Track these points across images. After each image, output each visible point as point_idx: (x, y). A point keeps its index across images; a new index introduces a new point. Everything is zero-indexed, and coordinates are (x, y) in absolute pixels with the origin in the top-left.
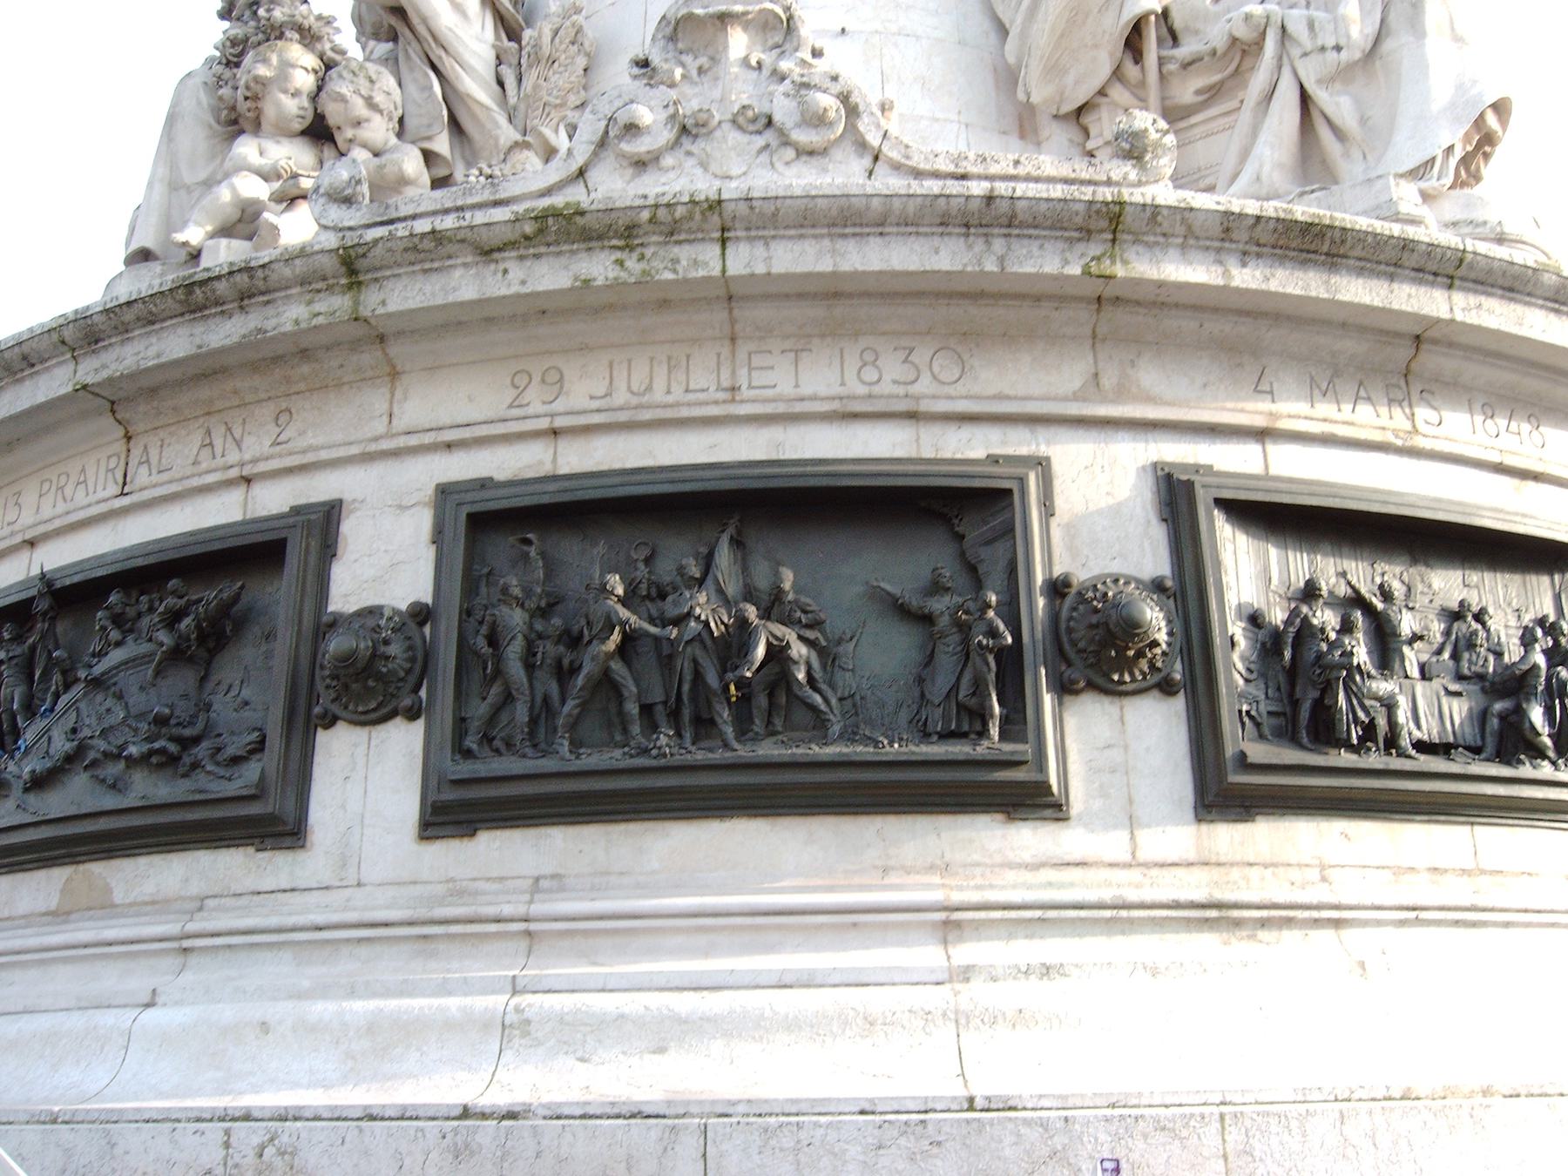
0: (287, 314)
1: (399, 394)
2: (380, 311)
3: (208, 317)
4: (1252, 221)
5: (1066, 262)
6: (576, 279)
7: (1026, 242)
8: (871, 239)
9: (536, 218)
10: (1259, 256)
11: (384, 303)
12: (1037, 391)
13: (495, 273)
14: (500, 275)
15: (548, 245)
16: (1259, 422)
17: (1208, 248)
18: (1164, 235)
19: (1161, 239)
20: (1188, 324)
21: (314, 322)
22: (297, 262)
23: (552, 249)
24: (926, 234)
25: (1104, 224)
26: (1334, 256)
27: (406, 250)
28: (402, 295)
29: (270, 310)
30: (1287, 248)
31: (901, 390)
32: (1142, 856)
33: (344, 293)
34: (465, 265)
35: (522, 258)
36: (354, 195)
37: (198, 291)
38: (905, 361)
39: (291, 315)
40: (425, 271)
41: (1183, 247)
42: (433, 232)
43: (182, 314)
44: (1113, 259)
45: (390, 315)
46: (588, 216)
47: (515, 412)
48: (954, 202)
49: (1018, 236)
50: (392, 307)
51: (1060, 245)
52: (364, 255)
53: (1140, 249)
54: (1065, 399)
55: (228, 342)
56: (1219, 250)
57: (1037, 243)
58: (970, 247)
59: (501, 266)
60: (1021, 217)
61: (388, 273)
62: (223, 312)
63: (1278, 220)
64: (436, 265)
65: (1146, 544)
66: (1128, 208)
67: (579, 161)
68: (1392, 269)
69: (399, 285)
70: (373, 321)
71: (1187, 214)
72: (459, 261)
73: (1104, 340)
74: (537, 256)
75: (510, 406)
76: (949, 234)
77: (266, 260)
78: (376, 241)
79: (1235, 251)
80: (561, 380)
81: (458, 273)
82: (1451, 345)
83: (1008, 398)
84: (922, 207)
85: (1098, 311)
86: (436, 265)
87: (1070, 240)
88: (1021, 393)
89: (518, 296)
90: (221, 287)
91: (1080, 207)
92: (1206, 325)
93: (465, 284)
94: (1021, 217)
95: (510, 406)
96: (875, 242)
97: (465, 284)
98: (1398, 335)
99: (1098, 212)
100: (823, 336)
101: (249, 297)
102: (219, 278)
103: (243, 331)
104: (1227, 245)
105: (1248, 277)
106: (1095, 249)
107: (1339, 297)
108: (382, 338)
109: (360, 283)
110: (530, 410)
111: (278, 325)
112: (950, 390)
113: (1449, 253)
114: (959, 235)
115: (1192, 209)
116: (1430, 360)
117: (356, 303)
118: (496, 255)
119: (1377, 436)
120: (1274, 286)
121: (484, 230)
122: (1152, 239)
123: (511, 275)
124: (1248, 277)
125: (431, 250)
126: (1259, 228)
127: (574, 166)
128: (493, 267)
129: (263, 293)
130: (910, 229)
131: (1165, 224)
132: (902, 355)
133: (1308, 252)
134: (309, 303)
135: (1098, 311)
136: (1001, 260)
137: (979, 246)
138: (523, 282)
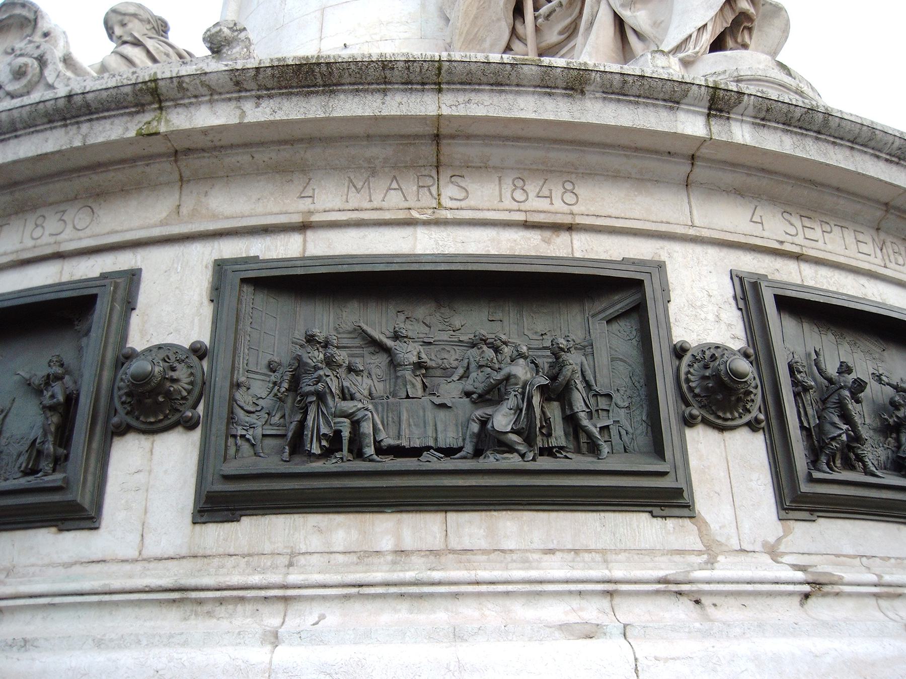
4: (253, 73)
5: (127, 129)
7: (102, 122)
8: (11, 141)
10: (270, 97)
12: (136, 223)
16: (297, 219)
17: (230, 99)
18: (196, 97)
19: (193, 100)
20: (242, 158)
24: (42, 131)
25: (149, 98)
26: (330, 85)
30: (291, 87)
31: (52, 240)
32: (146, 553)
38: (61, 220)
41: (211, 102)
44: (159, 121)
48: (48, 104)
49: (97, 119)
51: (125, 119)
53: (180, 110)
54: (155, 226)
56: (239, 99)
57: (109, 121)
58: (67, 133)
60: (93, 106)
63: (272, 67)
65: (196, 320)
66: (161, 83)
68: (383, 86)
71: (203, 78)
73: (189, 181)
76: (55, 127)
79: (252, 96)
82: (468, 137)
83: (117, 232)
84: (31, 113)
85: (176, 161)
87: (131, 114)
88: (125, 228)
91: (128, 90)
92: (256, 156)
94: (93, 106)
96: (13, 142)
98: (417, 136)
99: (141, 90)
100: (17, 213)
104: (243, 94)
105: (259, 113)
106: (148, 117)
107: (335, 114)
112: (81, 234)
113: (426, 65)
114: (61, 126)
115: (206, 73)
116: (454, 151)
119: (401, 215)
120: (279, 116)
122: (186, 101)
124: (259, 113)
126: (261, 76)
130: (32, 130)
131: (191, 88)
132: (59, 216)
133: (309, 86)
135: (176, 161)
136: (85, 137)
137: (73, 130)
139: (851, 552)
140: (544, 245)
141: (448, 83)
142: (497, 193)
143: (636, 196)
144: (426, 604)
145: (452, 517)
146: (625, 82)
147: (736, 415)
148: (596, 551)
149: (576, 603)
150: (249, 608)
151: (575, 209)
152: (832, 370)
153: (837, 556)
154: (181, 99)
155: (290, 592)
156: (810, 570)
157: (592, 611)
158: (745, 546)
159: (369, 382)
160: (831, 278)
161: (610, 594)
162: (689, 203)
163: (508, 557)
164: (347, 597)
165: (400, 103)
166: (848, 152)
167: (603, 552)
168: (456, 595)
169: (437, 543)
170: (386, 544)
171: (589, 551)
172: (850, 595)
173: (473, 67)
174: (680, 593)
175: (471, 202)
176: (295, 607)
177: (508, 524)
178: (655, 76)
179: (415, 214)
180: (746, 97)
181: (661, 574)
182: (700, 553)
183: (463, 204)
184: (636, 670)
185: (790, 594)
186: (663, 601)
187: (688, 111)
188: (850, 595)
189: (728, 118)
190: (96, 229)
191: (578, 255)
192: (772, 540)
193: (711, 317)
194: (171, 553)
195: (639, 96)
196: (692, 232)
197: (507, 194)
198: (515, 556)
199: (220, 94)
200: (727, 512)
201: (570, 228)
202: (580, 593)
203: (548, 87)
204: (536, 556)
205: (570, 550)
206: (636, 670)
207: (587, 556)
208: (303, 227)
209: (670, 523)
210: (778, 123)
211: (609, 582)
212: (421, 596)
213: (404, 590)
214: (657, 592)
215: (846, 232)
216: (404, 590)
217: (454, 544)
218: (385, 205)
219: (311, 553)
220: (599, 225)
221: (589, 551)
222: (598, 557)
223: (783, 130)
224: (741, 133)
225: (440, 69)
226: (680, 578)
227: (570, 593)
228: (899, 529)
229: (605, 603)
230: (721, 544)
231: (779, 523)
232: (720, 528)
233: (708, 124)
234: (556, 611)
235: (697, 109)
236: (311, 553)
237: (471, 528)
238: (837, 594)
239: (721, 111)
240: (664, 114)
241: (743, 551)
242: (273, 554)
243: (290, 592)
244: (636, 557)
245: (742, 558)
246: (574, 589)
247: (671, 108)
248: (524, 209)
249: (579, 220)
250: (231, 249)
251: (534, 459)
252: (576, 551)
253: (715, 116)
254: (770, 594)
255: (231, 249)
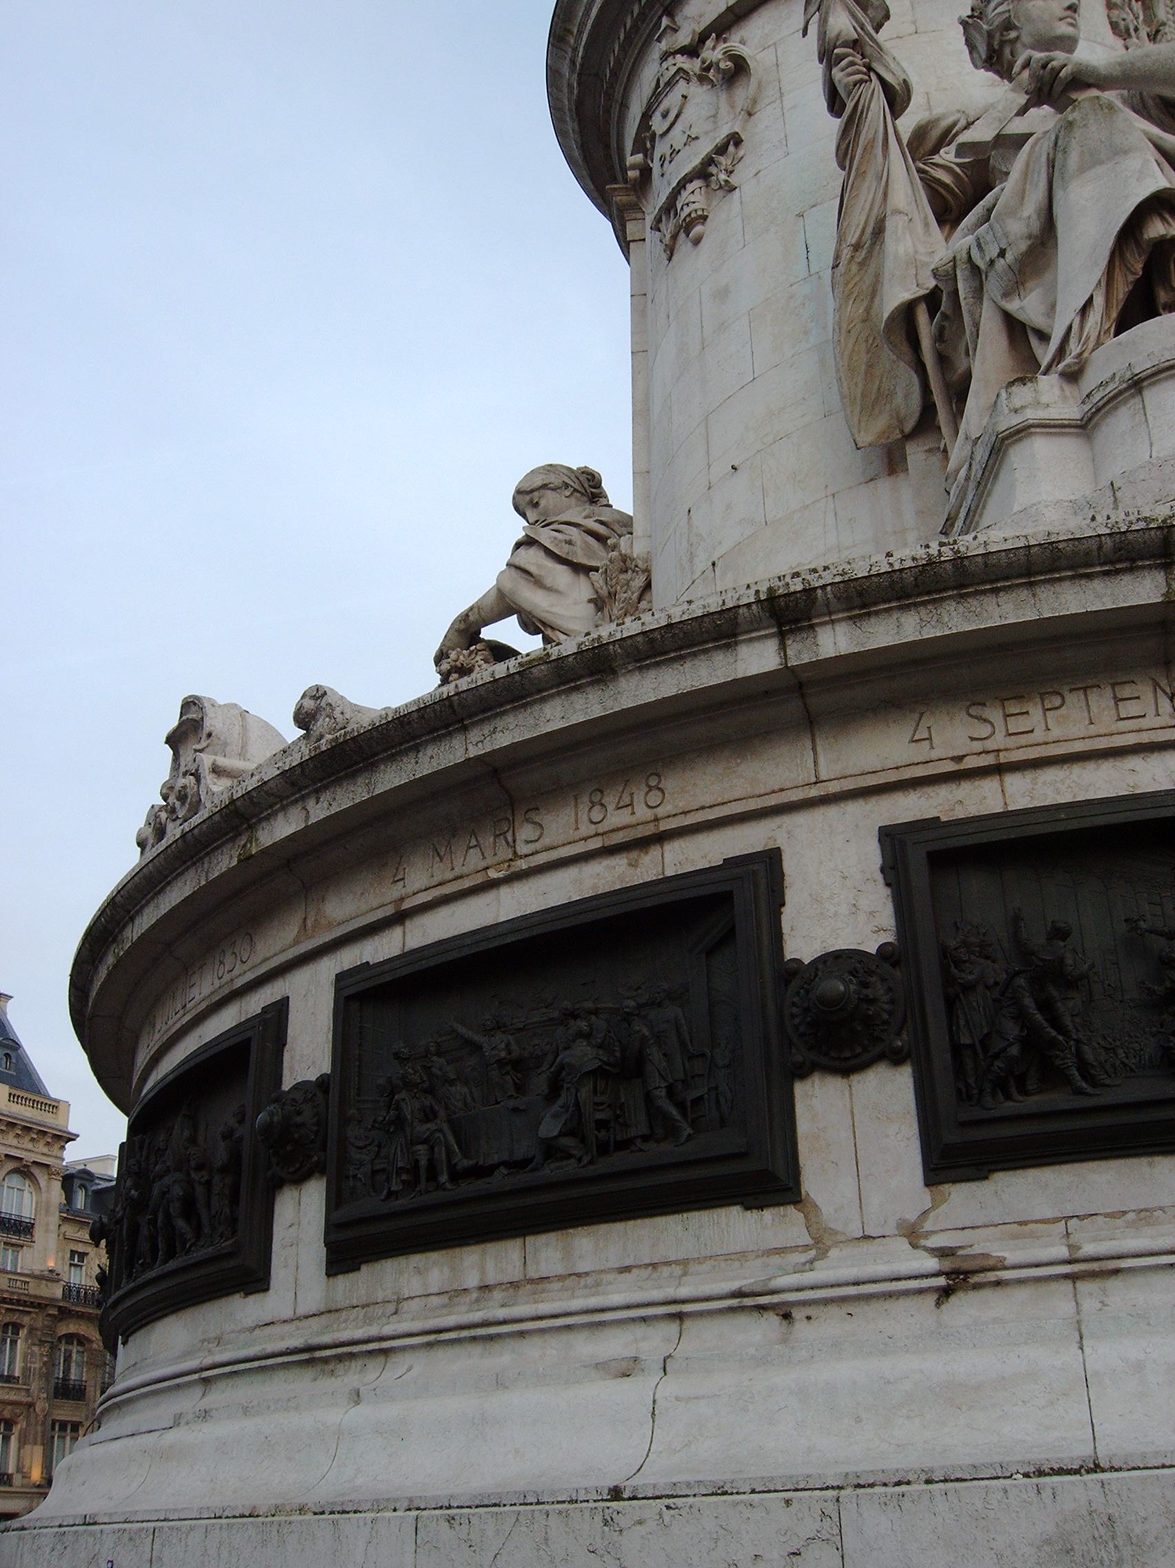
4: (299, 770)
105: (319, 810)
124: (319, 810)
139: (1049, 1214)
140: (631, 870)
141: (470, 717)
142: (573, 819)
143: (738, 765)
144: (496, 1346)
145: (530, 1240)
146: (652, 641)
147: (859, 1050)
148: (677, 1262)
149: (640, 1330)
150: (360, 1362)
151: (660, 811)
152: (1037, 938)
153: (1021, 1223)
154: (262, 812)
155: (385, 1345)
156: (960, 1252)
157: (653, 1342)
158: (870, 1231)
159: (465, 1090)
160: (1063, 781)
161: (680, 1317)
162: (814, 749)
163: (582, 1281)
164: (429, 1345)
165: (432, 757)
166: (1024, 594)
167: (685, 1263)
168: (522, 1334)
169: (515, 1273)
170: (472, 1280)
171: (668, 1263)
172: (1020, 1282)
173: (482, 691)
174: (761, 1308)
175: (546, 841)
176: (396, 1359)
177: (584, 1241)
178: (685, 617)
179: (493, 874)
180: (819, 591)
181: (734, 1285)
182: (807, 1248)
183: (538, 846)
184: (653, 1413)
185: (920, 1291)
186: (742, 1320)
187: (751, 640)
188: (1020, 1282)
189: (812, 627)
190: (256, 959)
191: (670, 872)
192: (912, 1216)
193: (844, 909)
194: (314, 1310)
195: (681, 648)
196: (814, 792)
197: (584, 817)
198: (589, 1280)
199: (288, 797)
200: (847, 1187)
201: (661, 838)
202: (644, 1319)
203: (572, 681)
204: (610, 1277)
205: (647, 1266)
206: (653, 1413)
207: (665, 1271)
208: (400, 918)
209: (768, 1214)
210: (890, 601)
211: (675, 1302)
212: (491, 1338)
213: (473, 1332)
214: (732, 1310)
215: (1093, 696)
216: (473, 1332)
217: (533, 1273)
218: (465, 870)
219: (412, 1298)
220: (690, 823)
221: (668, 1263)
222: (677, 1270)
223: (900, 608)
224: (835, 641)
225: (451, 706)
226: (758, 1289)
227: (633, 1320)
228: (1150, 1164)
229: (673, 1328)
230: (837, 1233)
231: (926, 1190)
232: (836, 1211)
233: (783, 647)
234: (615, 1344)
235: (763, 633)
236: (412, 1298)
237: (548, 1252)
238: (998, 1283)
239: (797, 621)
240: (719, 658)
241: (867, 1237)
242: (384, 1302)
243: (385, 1345)
244: (723, 1264)
245: (866, 1247)
246: (640, 1315)
247: (727, 646)
248: (600, 831)
249: (665, 826)
250: (349, 958)
251: (591, 1162)
252: (654, 1266)
253: (791, 631)
254: (889, 1295)
255: (349, 958)
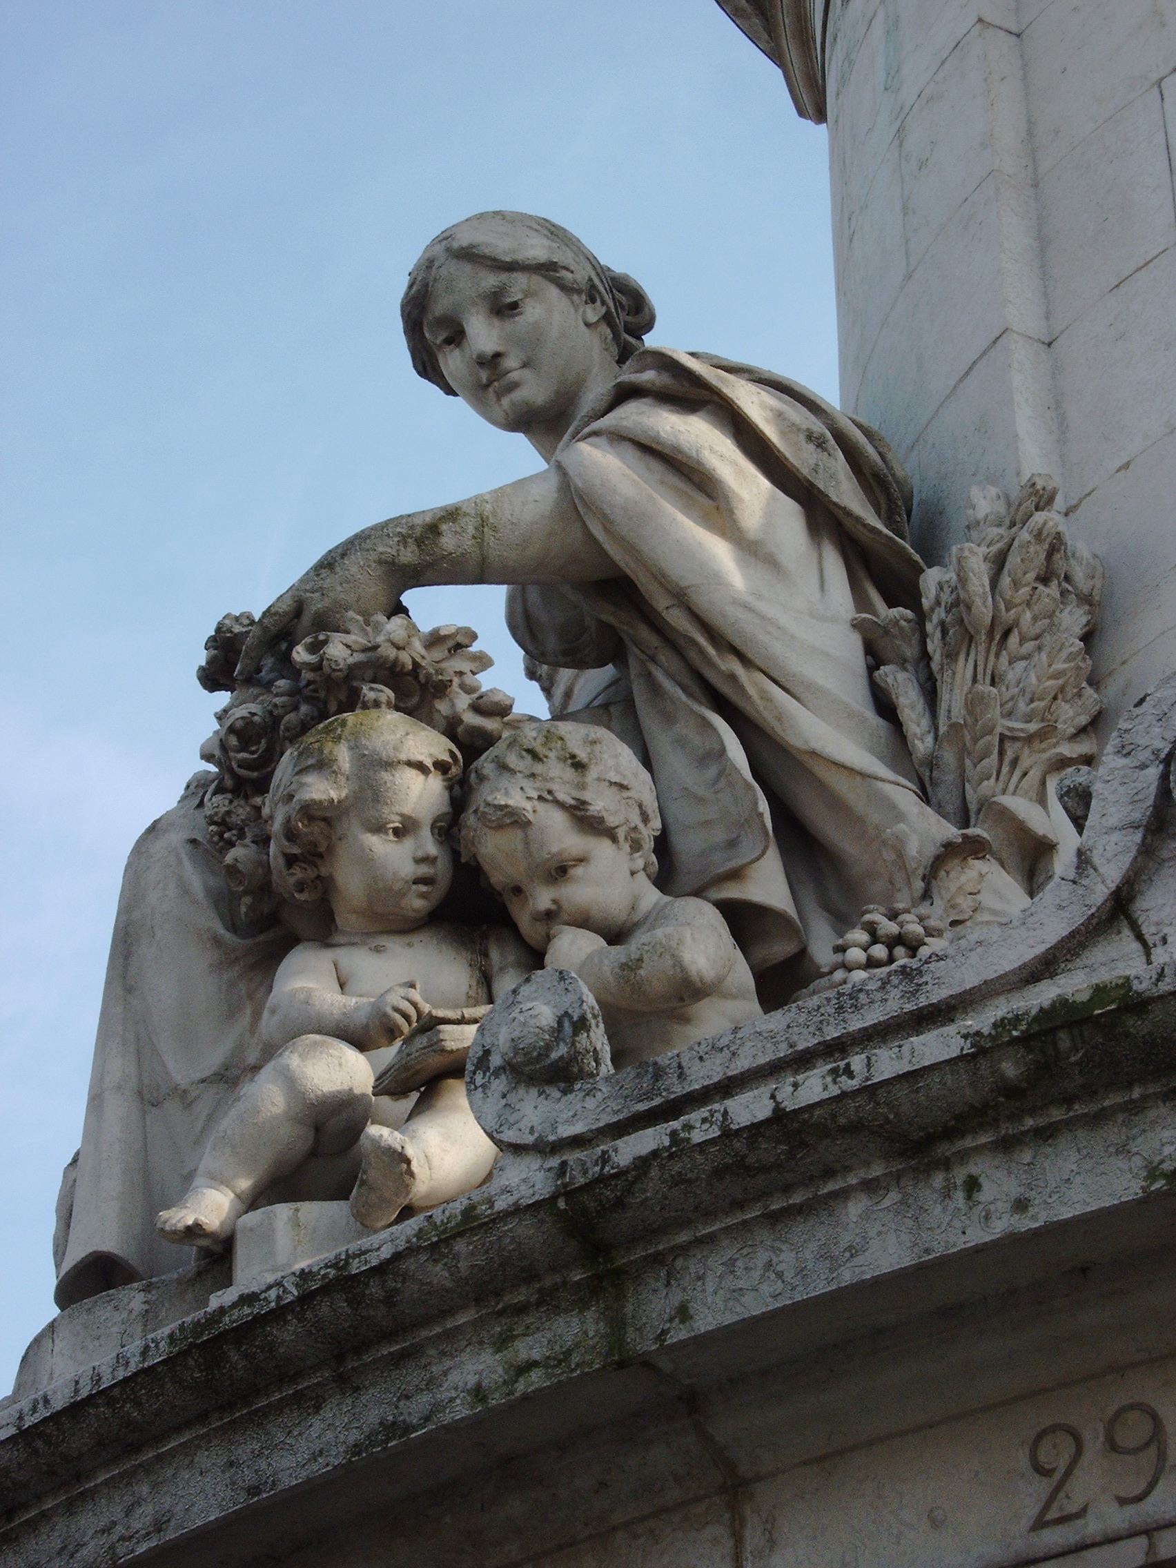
0: (454, 1378)
1: (753, 1537)
2: (679, 1334)
3: (264, 1413)
6: (1153, 1173)
9: (1025, 1040)
11: (684, 1313)
13: (947, 1193)
14: (959, 1195)
15: (1068, 1101)
21: (521, 1387)
22: (461, 1246)
23: (1079, 1109)
27: (719, 1173)
28: (733, 1287)
29: (414, 1377)
33: (584, 1306)
34: (870, 1187)
35: (1006, 1146)
36: (574, 1057)
37: (234, 1356)
39: (466, 1375)
40: (773, 1219)
42: (779, 1115)
43: (203, 1417)
45: (702, 1341)
46: (1157, 1013)
47: (1054, 1537)
50: (705, 1321)
52: (619, 1204)
55: (318, 1468)
59: (959, 1175)
61: (683, 1237)
62: (298, 1398)
64: (797, 1198)
67: (1111, 871)
69: (716, 1263)
70: (665, 1364)
72: (853, 1180)
74: (1046, 1134)
75: (1040, 1524)
77: (386, 1253)
78: (643, 1164)
80: (1157, 1436)
81: (855, 1209)
86: (797, 1198)
89: (1013, 1240)
90: (287, 1334)
93: (878, 1236)
95: (1040, 1524)
97: (878, 1236)
101: (358, 1351)
102: (279, 1314)
103: (354, 1436)
108: (691, 1403)
109: (619, 1273)
110: (1092, 1527)
111: (437, 1407)
117: (617, 1324)
118: (944, 1149)
121: (901, 1091)
123: (987, 1193)
125: (784, 1167)
127: (1100, 892)
128: (938, 1180)
129: (388, 1336)
134: (503, 1342)
138: (1021, 1205)
